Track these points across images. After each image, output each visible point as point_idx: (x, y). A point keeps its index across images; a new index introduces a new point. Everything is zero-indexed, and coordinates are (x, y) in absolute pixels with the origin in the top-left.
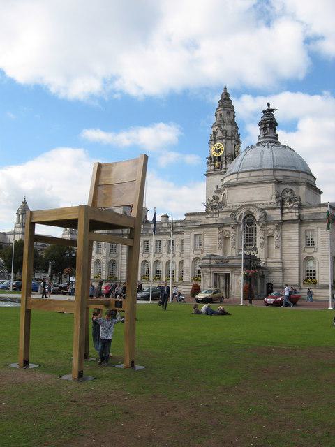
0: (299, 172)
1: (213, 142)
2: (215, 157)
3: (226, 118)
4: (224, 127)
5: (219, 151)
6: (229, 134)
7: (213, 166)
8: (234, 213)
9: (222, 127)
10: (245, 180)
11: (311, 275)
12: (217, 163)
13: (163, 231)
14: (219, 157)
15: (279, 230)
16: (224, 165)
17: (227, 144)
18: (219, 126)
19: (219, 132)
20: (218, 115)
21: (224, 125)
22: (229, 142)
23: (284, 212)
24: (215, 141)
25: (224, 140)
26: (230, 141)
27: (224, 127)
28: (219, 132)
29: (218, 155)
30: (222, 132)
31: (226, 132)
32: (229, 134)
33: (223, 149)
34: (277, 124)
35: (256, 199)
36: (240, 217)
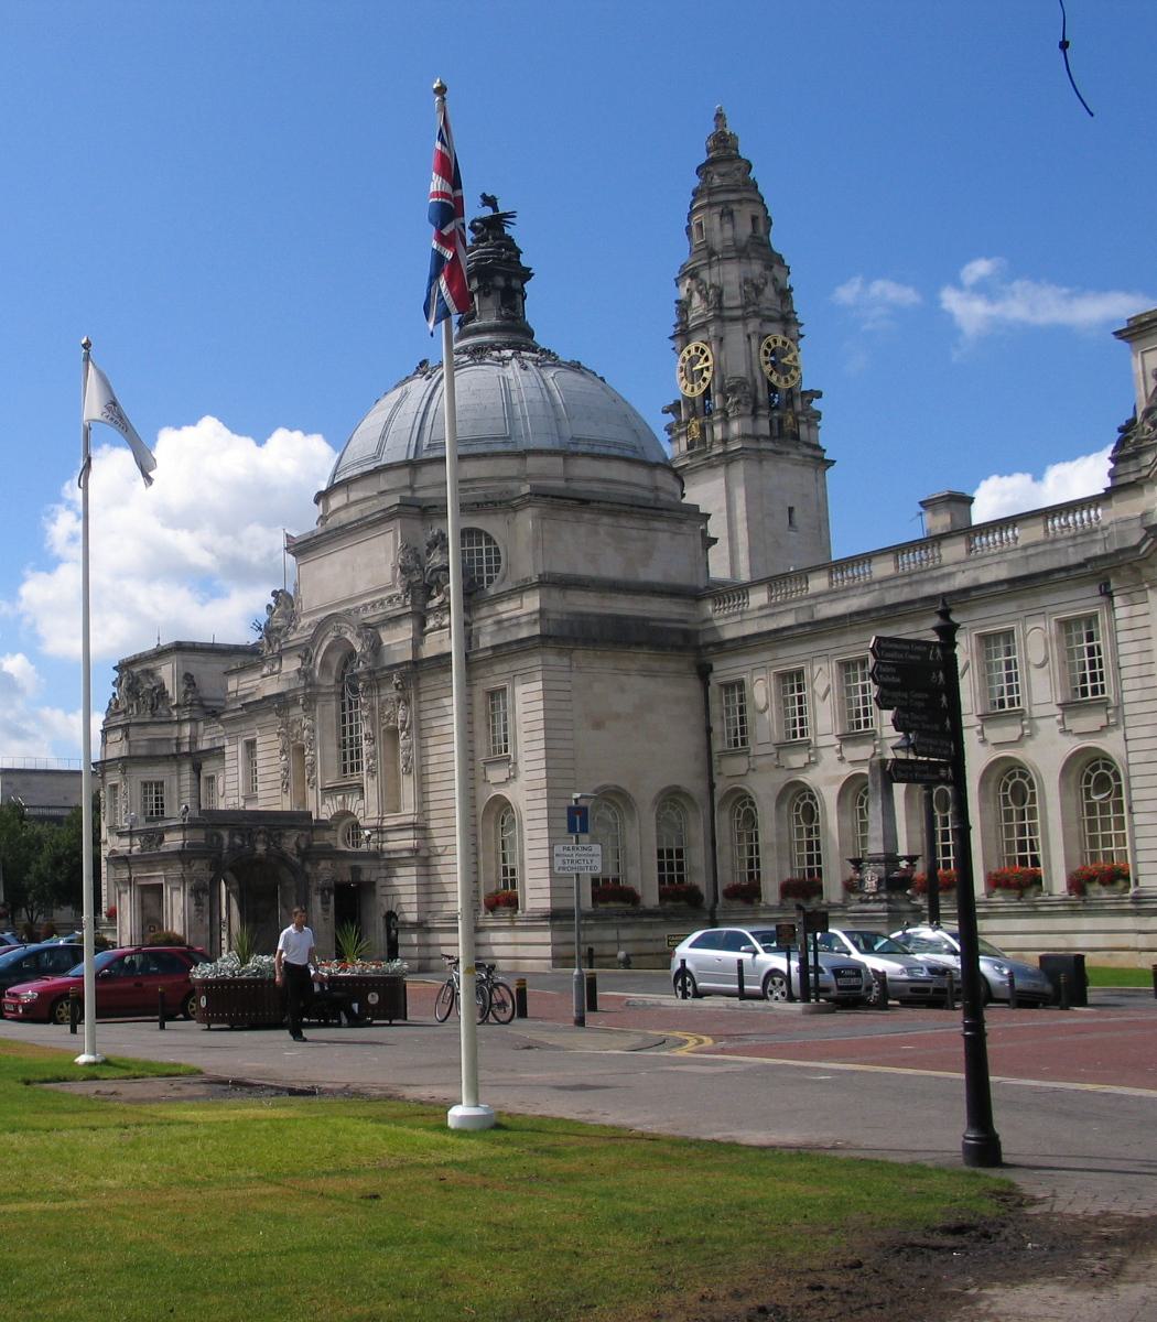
0: (523, 455)
3: (720, 234)
6: (733, 299)
8: (305, 652)
10: (353, 514)
15: (407, 703)
19: (696, 300)
20: (694, 229)
21: (709, 265)
22: (736, 334)
23: (431, 623)
26: (739, 326)
28: (696, 300)
29: (698, 392)
30: (705, 298)
31: (720, 295)
32: (733, 299)
34: (526, 274)
35: (361, 588)
36: (324, 664)
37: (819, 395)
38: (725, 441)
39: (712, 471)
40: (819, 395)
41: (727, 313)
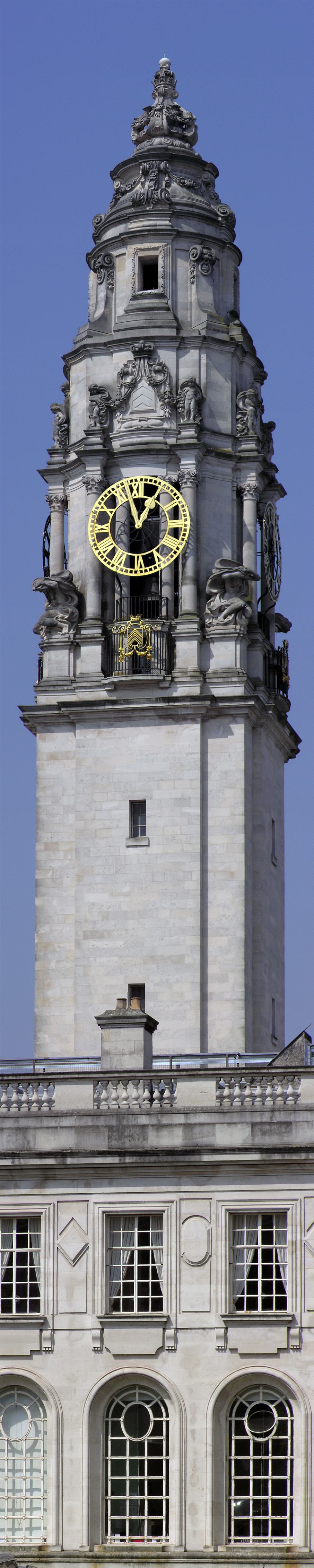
1: (94, 471)
2: (106, 579)
4: (189, 365)
5: (141, 540)
7: (91, 656)
9: (166, 356)
11: (137, 1487)
12: (130, 631)
13: (173, 1139)
14: (139, 586)
16: (187, 652)
17: (209, 486)
18: (145, 353)
19: (144, 396)
21: (180, 343)
24: (111, 462)
25: (188, 464)
27: (189, 365)
28: (144, 396)
29: (140, 570)
33: (184, 523)
37: (285, 627)
38: (202, 674)
39: (175, 728)
40: (285, 627)
41: (209, 440)
